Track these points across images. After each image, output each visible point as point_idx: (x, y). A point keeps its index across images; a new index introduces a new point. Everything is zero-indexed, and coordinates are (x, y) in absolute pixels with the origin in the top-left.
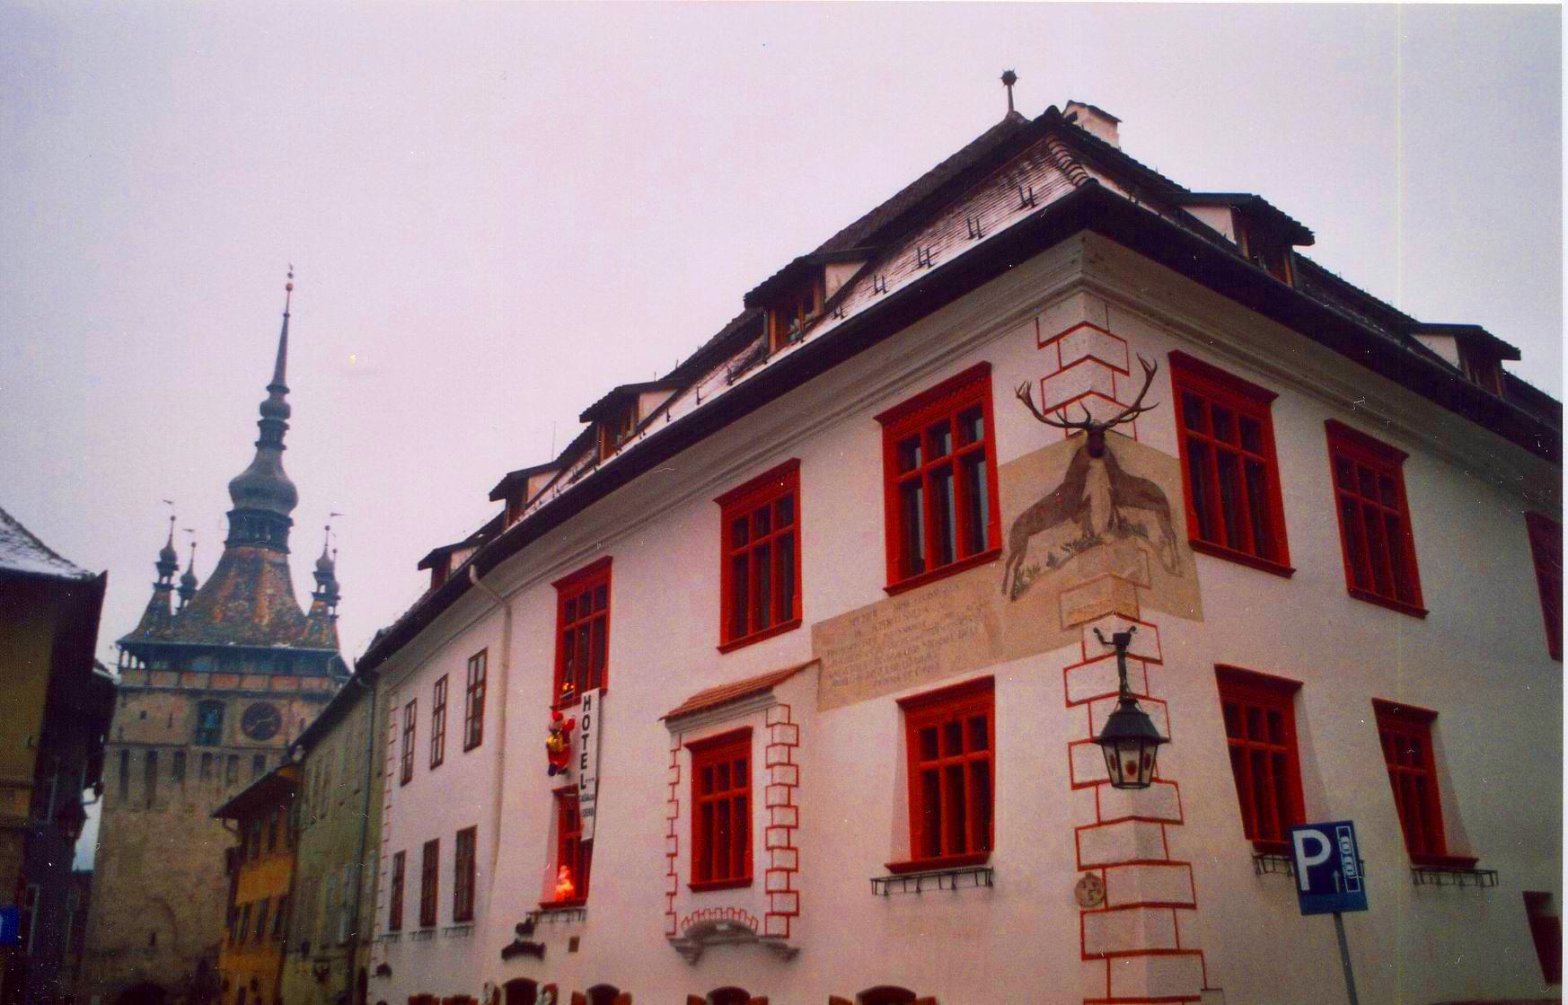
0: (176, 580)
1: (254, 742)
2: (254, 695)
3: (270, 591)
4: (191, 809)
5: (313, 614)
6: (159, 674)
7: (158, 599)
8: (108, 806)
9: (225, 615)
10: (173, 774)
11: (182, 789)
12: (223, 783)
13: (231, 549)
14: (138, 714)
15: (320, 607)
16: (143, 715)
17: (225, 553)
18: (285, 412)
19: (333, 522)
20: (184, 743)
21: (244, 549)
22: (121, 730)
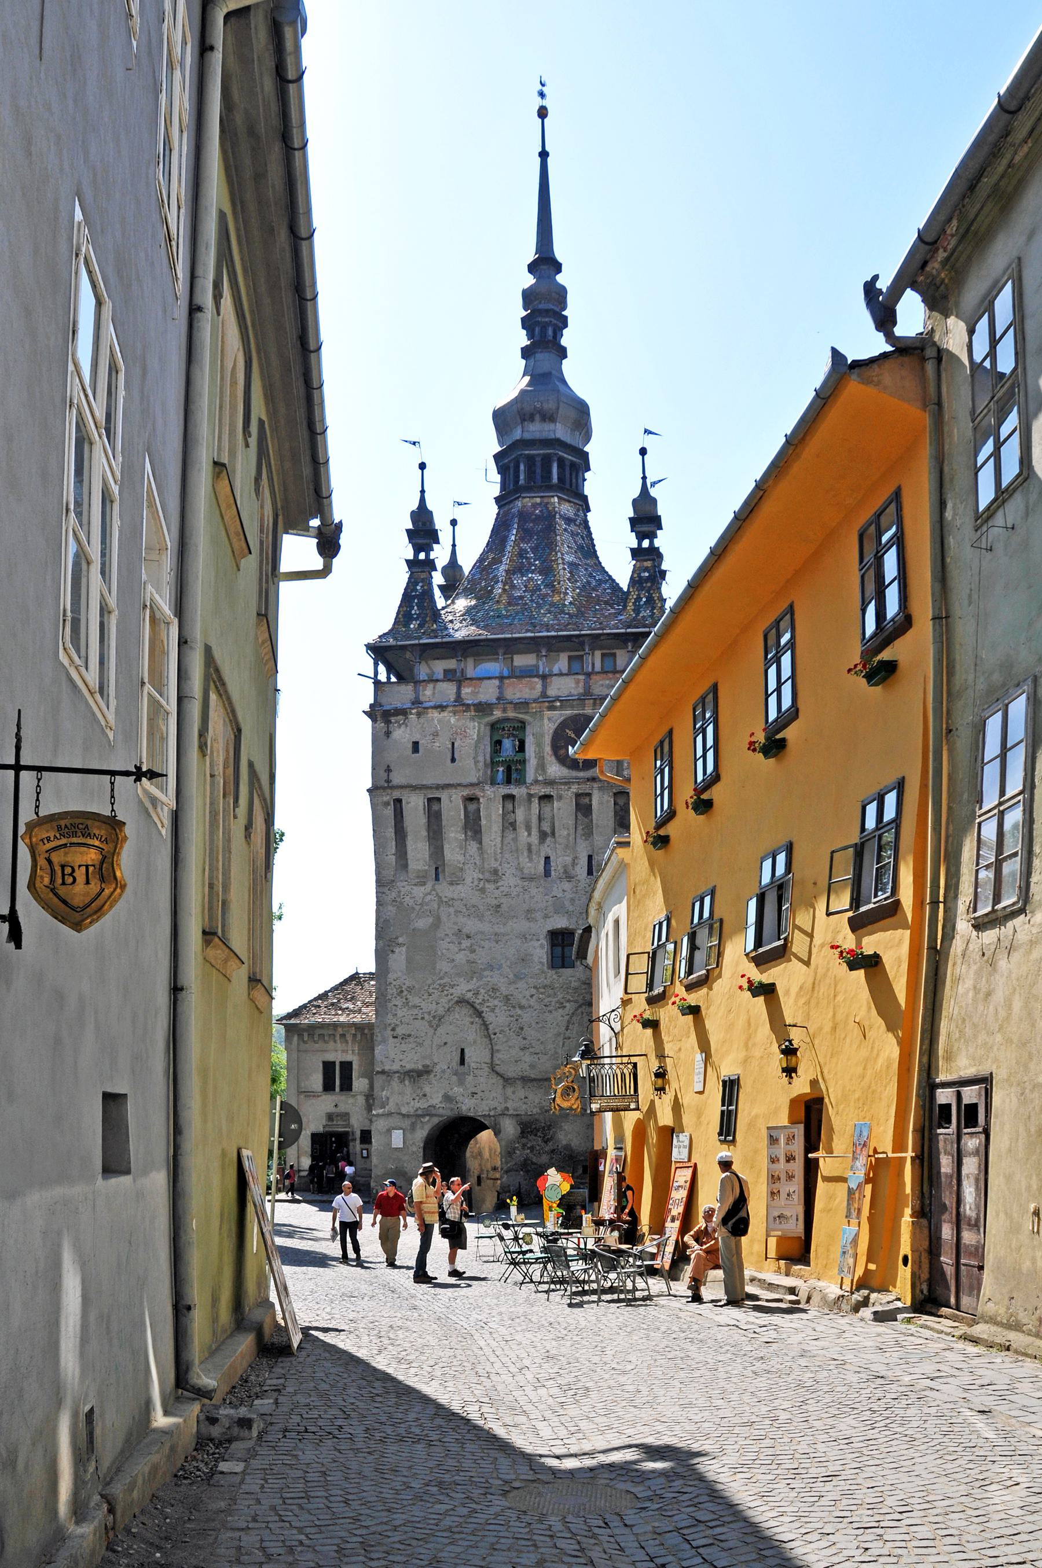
0: (440, 555)
1: (575, 774)
3: (569, 558)
6: (431, 686)
9: (511, 597)
10: (466, 827)
11: (480, 849)
12: (535, 839)
14: (410, 745)
20: (475, 780)
21: (525, 502)
22: (388, 770)
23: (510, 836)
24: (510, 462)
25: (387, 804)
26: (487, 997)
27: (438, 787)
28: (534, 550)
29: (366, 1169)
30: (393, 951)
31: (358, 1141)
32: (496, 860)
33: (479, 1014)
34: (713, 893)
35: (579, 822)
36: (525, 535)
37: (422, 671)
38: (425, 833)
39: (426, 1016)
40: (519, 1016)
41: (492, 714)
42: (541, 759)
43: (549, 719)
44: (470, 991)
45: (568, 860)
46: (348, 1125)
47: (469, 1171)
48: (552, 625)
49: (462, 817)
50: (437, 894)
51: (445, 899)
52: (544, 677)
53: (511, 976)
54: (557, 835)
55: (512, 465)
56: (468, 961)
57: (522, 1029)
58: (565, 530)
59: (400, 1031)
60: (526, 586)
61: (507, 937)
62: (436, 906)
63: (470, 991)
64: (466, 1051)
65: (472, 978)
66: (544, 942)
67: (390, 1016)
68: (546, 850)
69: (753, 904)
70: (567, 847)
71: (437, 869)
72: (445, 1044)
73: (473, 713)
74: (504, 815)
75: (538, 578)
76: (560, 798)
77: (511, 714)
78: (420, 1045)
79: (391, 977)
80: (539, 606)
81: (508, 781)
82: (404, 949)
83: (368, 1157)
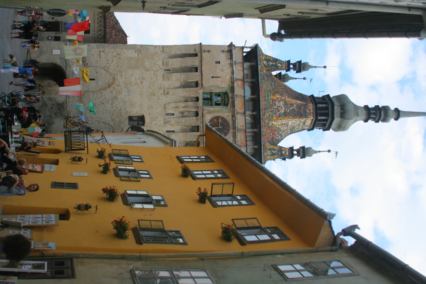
2: (234, 121)
3: (290, 123)
4: (166, 92)
5: (281, 149)
6: (242, 69)
7: (281, 64)
8: (165, 48)
9: (276, 100)
11: (177, 88)
12: (181, 109)
13: (309, 99)
14: (218, 60)
15: (285, 153)
17: (307, 96)
18: (384, 120)
19: (333, 153)
20: (204, 85)
21: (311, 106)
22: (209, 51)
23: (182, 100)
24: (326, 101)
26: (116, 90)
27: (201, 71)
29: (43, 38)
30: (136, 51)
31: (56, 35)
32: (173, 94)
33: (109, 86)
34: (151, 178)
35: (188, 127)
36: (299, 107)
37: (246, 65)
38: (183, 65)
39: (108, 65)
40: (109, 103)
41: (230, 93)
43: (228, 115)
44: (119, 83)
45: (173, 123)
47: (43, 81)
48: (264, 117)
49: (190, 81)
50: (159, 70)
52: (245, 113)
53: (125, 100)
54: (182, 118)
55: (325, 101)
56: (131, 82)
57: (103, 104)
58: (301, 122)
59: (102, 54)
60: (279, 106)
61: (141, 98)
62: (154, 69)
63: (119, 83)
64: (94, 81)
65: (125, 84)
66: (139, 114)
67: (109, 50)
68: (177, 113)
69: (145, 193)
70: (178, 122)
71: (169, 70)
73: (231, 85)
74: (191, 97)
75: (283, 111)
76: (197, 120)
77: (230, 100)
78: (96, 63)
79: (125, 50)
80: (272, 111)
81: (204, 99)
82: (137, 56)
83: (48, 39)
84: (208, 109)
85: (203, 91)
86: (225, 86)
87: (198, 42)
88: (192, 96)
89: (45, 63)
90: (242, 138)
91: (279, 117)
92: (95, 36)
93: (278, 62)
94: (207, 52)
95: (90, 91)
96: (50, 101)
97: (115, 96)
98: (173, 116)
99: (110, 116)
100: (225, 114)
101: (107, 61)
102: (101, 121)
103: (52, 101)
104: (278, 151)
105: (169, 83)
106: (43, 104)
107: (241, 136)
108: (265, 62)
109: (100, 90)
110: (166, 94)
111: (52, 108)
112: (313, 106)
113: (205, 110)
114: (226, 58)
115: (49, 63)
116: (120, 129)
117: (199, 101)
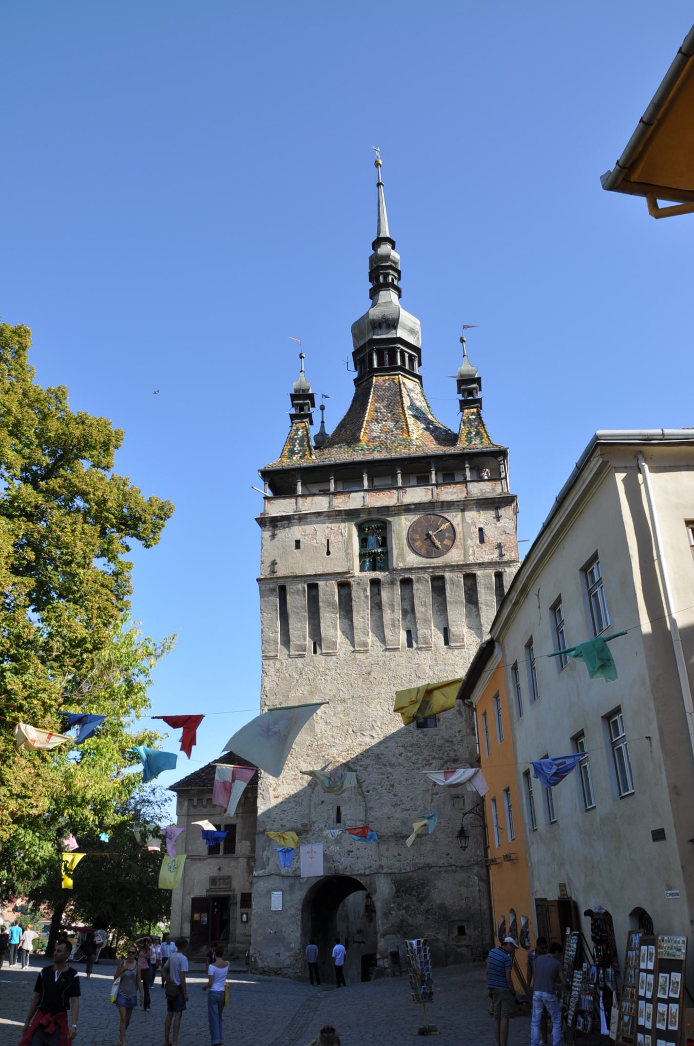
6: (309, 499)
7: (298, 430)
12: (399, 614)
15: (473, 414)
16: (298, 544)
20: (345, 570)
22: (274, 563)
25: (273, 590)
27: (315, 575)
28: (387, 407)
31: (239, 905)
40: (390, 773)
42: (401, 550)
46: (230, 889)
51: (323, 670)
54: (416, 612)
57: (392, 786)
72: (323, 802)
73: (344, 517)
75: (391, 424)
76: (419, 579)
77: (375, 516)
78: (300, 804)
81: (374, 568)
83: (247, 922)
84: (394, 559)
85: (358, 569)
86: (345, 527)
87: (257, 585)
88: (369, 593)
89: (303, 929)
90: (451, 490)
91: (403, 428)
92: (240, 812)
93: (294, 435)
94: (276, 567)
95: (364, 818)
96: (391, 914)
97: (373, 760)
98: (412, 632)
99: (418, 769)
100: (404, 525)
101: (295, 779)
102: (433, 789)
103: (391, 909)
104: (472, 426)
105: (342, 643)
106: (399, 933)
107: (447, 493)
108: (294, 458)
109: (362, 794)
110: (365, 649)
111: (407, 908)
112: (376, 376)
113: (397, 564)
114: (287, 529)
115: (302, 918)
116: (447, 744)
117: (379, 577)
